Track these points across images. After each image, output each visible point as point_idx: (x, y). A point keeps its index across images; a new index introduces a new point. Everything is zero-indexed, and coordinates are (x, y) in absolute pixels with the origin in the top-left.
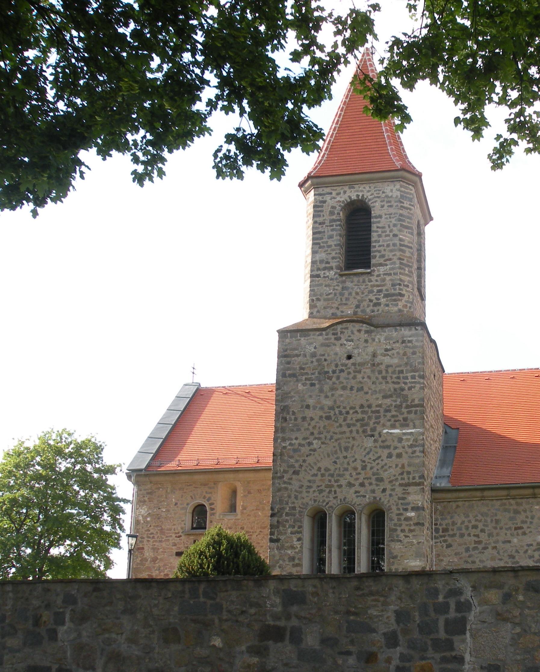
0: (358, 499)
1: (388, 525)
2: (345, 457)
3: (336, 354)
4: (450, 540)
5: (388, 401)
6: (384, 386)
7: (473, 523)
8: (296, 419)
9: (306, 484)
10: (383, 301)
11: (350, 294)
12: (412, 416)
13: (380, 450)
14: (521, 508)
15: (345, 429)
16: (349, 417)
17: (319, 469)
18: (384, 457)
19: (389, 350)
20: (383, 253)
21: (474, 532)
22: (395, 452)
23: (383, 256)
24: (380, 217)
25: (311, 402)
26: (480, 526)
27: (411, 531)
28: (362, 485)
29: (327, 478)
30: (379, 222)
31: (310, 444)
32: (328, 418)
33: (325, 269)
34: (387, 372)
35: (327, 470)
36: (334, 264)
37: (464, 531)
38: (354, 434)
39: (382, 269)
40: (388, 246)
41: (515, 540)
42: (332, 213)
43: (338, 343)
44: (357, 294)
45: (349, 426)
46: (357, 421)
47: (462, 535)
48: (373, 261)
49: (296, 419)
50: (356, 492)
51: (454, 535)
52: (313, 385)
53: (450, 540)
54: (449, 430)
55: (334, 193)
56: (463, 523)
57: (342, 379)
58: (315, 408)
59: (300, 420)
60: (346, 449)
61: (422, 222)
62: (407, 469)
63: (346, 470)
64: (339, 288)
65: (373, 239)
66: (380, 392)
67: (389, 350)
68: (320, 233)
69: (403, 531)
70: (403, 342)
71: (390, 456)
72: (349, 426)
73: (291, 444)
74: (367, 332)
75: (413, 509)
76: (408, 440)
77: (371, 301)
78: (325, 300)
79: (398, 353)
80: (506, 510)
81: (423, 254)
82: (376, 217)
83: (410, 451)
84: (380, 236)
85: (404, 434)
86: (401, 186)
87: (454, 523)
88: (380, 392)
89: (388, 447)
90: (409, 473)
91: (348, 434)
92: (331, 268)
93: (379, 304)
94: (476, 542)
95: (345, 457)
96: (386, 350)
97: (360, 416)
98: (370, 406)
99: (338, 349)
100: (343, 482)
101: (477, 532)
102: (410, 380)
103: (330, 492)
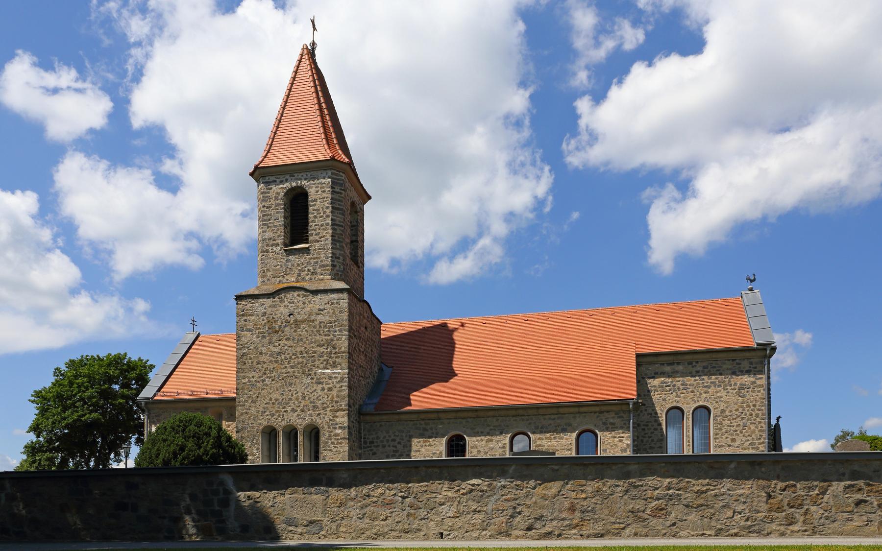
0: (300, 422)
1: (323, 439)
2: (290, 391)
3: (281, 313)
4: (375, 450)
5: (321, 349)
6: (318, 338)
7: (392, 437)
8: (252, 363)
9: (261, 409)
10: (319, 270)
11: (293, 265)
12: (339, 360)
13: (315, 385)
14: (428, 427)
15: (289, 370)
16: (292, 361)
17: (271, 399)
18: (319, 391)
19: (322, 310)
20: (318, 231)
21: (392, 444)
22: (326, 387)
23: (317, 234)
24: (316, 200)
25: (264, 350)
26: (398, 440)
27: (338, 443)
28: (303, 411)
29: (276, 406)
30: (314, 205)
31: (263, 381)
32: (277, 362)
33: (273, 245)
34: (320, 327)
35: (277, 400)
36: (279, 241)
37: (385, 443)
38: (296, 373)
39: (318, 245)
40: (322, 225)
41: (423, 450)
42: (276, 198)
43: (282, 305)
44: (298, 265)
45: (292, 367)
46: (298, 364)
47: (384, 446)
48: (310, 238)
49: (252, 363)
50: (298, 416)
51: (378, 446)
52: (264, 337)
53: (375, 450)
54: (385, 368)
55: (278, 181)
56: (385, 437)
57: (286, 333)
58: (266, 354)
59: (255, 363)
60: (291, 385)
61: (358, 201)
62: (336, 399)
63: (291, 399)
64: (284, 261)
65: (310, 220)
66: (315, 342)
67: (322, 310)
68: (267, 215)
69: (333, 443)
70: (333, 303)
71: (323, 389)
72: (292, 367)
73: (249, 381)
74: (305, 296)
75: (340, 428)
76: (336, 378)
77: (309, 270)
78: (274, 270)
79: (329, 312)
80: (417, 428)
81: (360, 229)
82: (312, 201)
83: (338, 385)
84: (315, 217)
85: (334, 373)
86: (332, 174)
87: (378, 438)
88: (315, 342)
89: (322, 383)
90: (337, 402)
91: (291, 374)
92: (278, 245)
93: (316, 273)
94: (394, 451)
95: (290, 391)
96: (320, 310)
97: (300, 360)
98: (307, 352)
99: (282, 309)
100: (289, 409)
101: (396, 443)
102: (338, 333)
103: (279, 415)
